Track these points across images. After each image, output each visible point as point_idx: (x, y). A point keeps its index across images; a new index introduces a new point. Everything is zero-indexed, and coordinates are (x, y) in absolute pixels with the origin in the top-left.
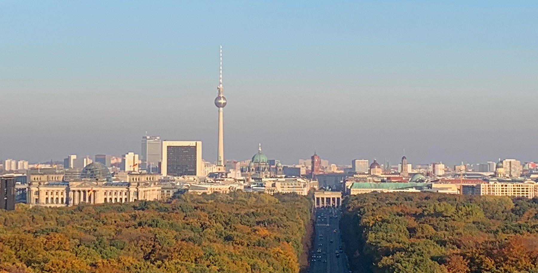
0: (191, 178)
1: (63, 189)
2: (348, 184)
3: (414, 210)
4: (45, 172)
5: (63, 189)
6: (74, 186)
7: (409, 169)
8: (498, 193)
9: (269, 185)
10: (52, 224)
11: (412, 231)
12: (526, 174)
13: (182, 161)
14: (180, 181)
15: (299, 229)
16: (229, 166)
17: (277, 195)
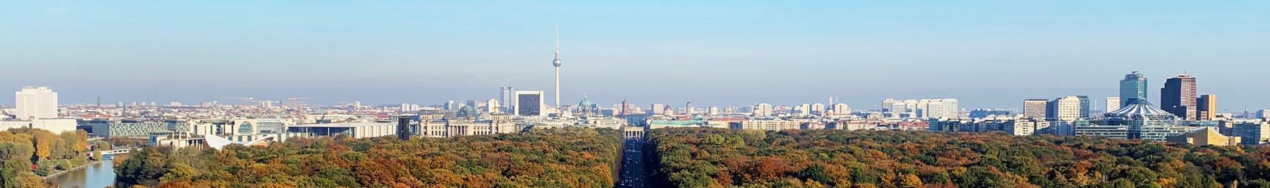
1: (443, 125)
2: (648, 122)
3: (694, 139)
4: (430, 112)
5: (443, 125)
6: (452, 122)
7: (692, 111)
8: (755, 128)
9: (592, 122)
10: (436, 150)
11: (693, 155)
12: (775, 114)
13: (530, 105)
14: (529, 120)
15: (613, 153)
16: (564, 107)
17: (598, 129)
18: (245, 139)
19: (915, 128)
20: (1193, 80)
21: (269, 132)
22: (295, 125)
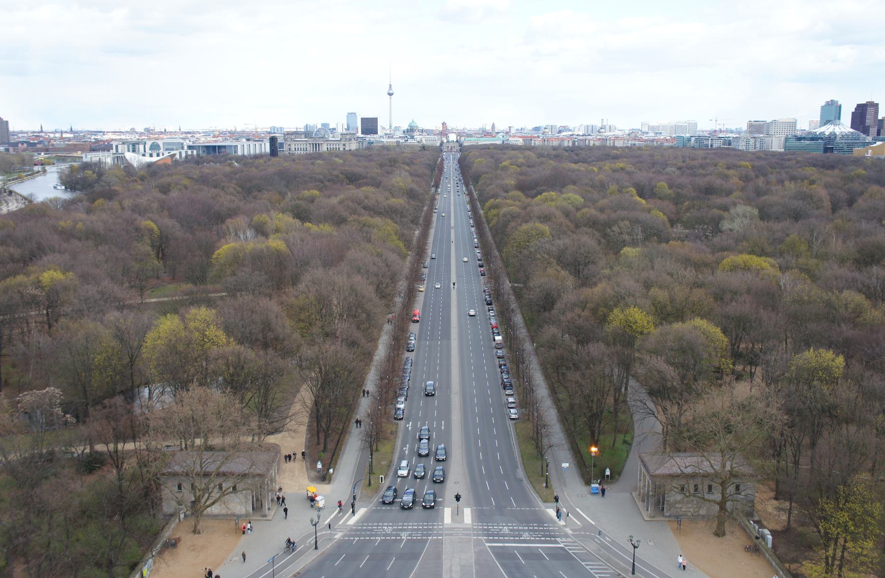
0: (375, 136)
13: (370, 126)
18: (155, 154)
19: (666, 144)
20: (877, 105)
21: (173, 150)
22: (191, 144)
